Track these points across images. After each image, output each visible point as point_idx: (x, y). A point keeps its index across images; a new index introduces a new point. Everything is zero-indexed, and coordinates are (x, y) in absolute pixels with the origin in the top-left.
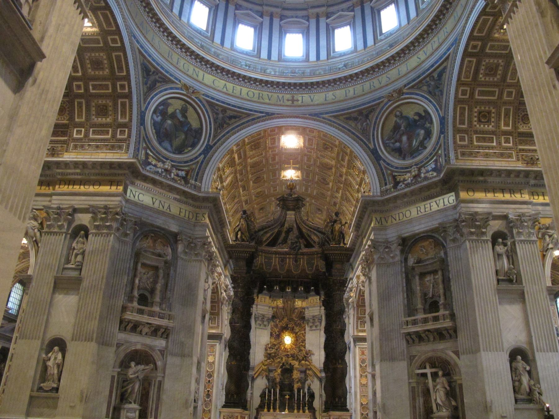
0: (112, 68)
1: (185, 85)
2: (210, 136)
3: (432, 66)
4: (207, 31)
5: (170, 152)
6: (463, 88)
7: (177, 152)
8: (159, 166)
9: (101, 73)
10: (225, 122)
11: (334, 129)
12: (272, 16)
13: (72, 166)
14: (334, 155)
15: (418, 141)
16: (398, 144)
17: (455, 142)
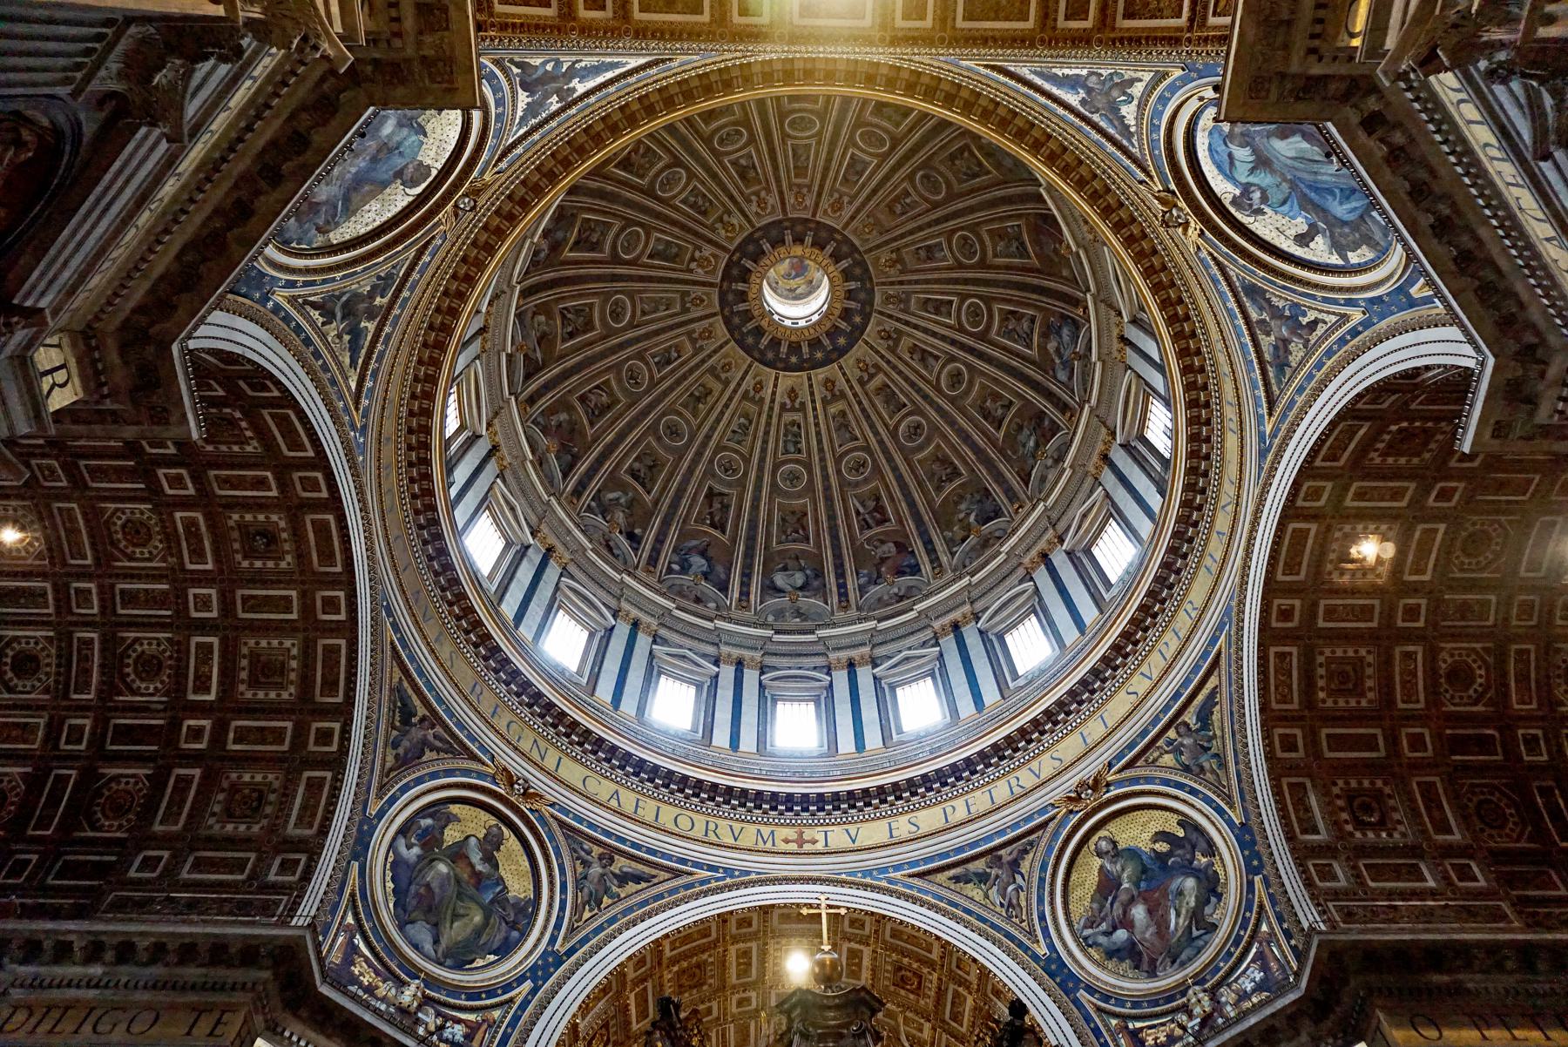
0: (306, 681)
1: (505, 769)
2: (558, 927)
3: (1177, 695)
4: (580, 673)
5: (427, 957)
6: (1281, 731)
7: (449, 962)
8: (381, 992)
9: (273, 695)
10: (607, 891)
11: (924, 910)
12: (740, 664)
13: (78, 955)
14: (927, 1003)
15: (1184, 911)
16: (1121, 935)
17: (1308, 884)
